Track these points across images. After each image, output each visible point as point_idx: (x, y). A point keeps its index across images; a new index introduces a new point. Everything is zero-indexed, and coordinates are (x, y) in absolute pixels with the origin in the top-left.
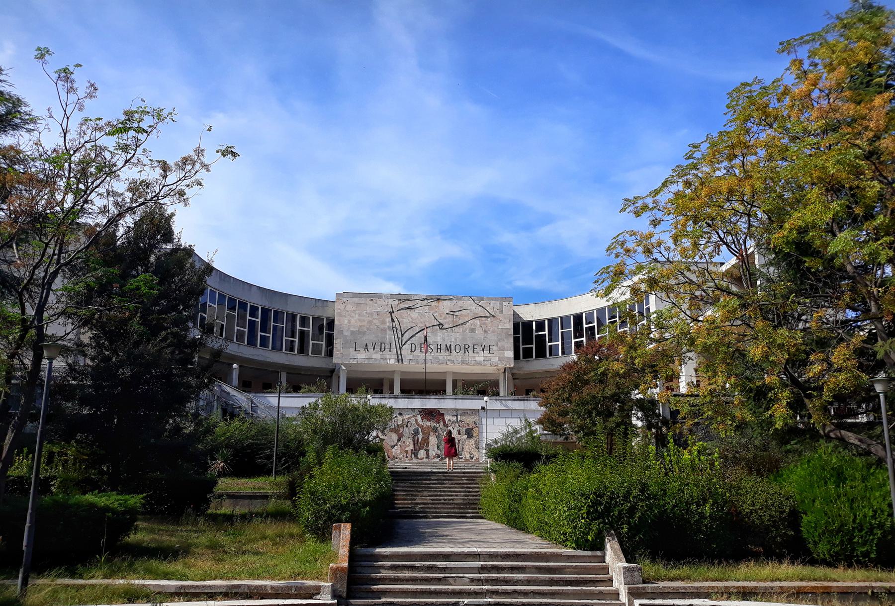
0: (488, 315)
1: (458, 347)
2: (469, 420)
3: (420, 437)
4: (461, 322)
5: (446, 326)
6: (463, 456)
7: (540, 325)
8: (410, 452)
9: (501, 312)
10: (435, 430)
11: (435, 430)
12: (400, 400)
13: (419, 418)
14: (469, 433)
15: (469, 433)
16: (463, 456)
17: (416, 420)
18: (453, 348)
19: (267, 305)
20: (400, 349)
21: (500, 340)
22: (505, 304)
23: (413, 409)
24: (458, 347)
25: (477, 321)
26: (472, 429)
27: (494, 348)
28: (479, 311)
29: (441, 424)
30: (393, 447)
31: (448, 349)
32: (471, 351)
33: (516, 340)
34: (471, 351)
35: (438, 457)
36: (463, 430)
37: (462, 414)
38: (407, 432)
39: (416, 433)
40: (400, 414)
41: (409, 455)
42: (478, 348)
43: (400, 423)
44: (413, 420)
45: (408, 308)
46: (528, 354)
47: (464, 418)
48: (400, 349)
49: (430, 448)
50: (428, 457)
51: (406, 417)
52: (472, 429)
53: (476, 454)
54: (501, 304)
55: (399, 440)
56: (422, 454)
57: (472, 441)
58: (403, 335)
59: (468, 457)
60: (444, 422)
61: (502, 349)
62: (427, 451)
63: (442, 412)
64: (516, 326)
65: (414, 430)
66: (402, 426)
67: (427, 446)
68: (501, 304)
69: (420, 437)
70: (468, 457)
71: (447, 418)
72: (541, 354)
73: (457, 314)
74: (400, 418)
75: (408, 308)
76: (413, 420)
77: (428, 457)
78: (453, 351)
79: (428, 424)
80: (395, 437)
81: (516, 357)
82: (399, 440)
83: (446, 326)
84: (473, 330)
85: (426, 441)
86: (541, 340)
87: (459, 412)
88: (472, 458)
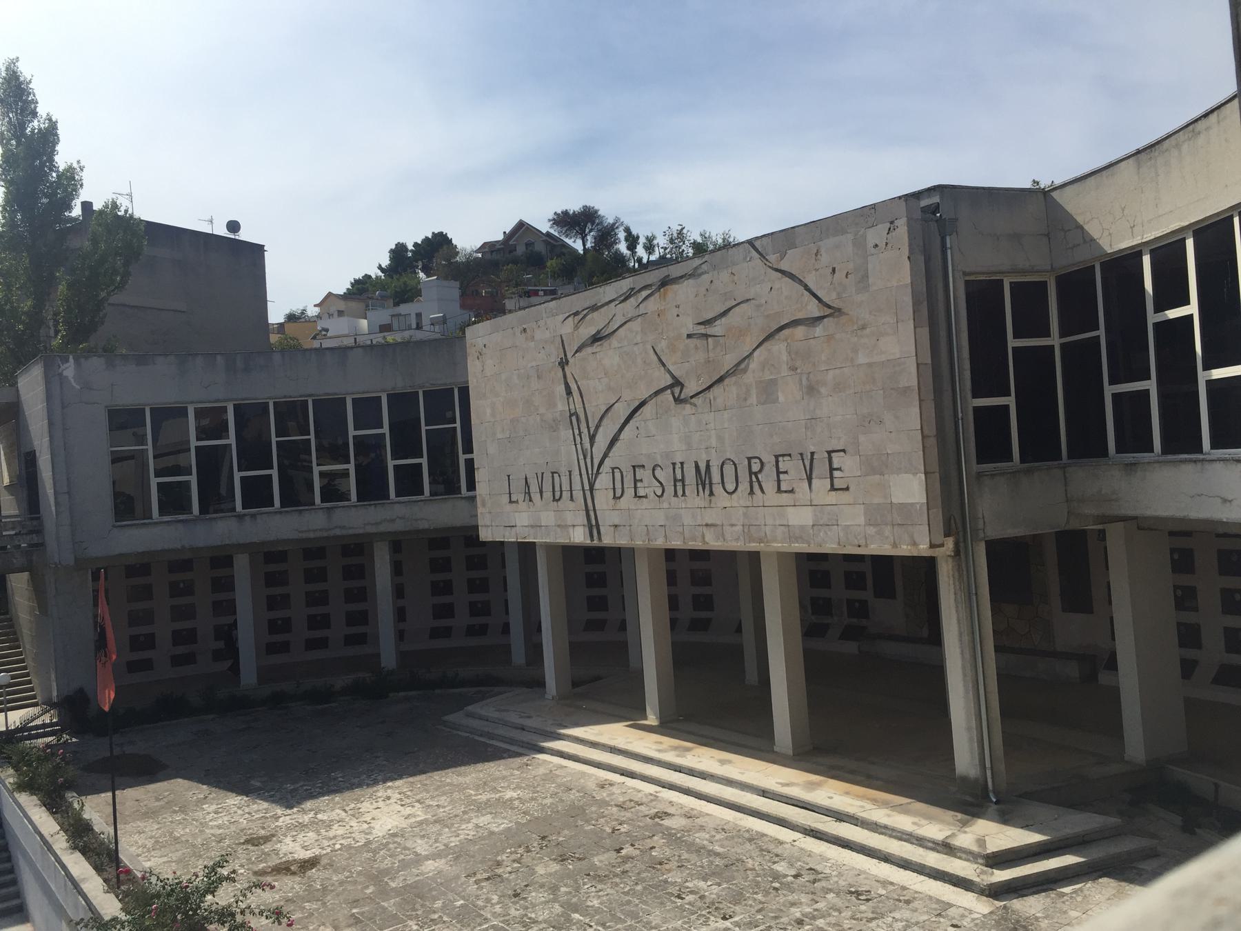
0: (814, 309)
4: (729, 361)
5: (692, 387)
18: (716, 477)
19: (400, 384)
20: (591, 489)
25: (778, 348)
31: (704, 479)
45: (596, 338)
48: (591, 489)
54: (859, 243)
58: (592, 438)
61: (878, 466)
68: (859, 243)
73: (717, 329)
75: (596, 338)
78: (718, 489)
83: (692, 387)
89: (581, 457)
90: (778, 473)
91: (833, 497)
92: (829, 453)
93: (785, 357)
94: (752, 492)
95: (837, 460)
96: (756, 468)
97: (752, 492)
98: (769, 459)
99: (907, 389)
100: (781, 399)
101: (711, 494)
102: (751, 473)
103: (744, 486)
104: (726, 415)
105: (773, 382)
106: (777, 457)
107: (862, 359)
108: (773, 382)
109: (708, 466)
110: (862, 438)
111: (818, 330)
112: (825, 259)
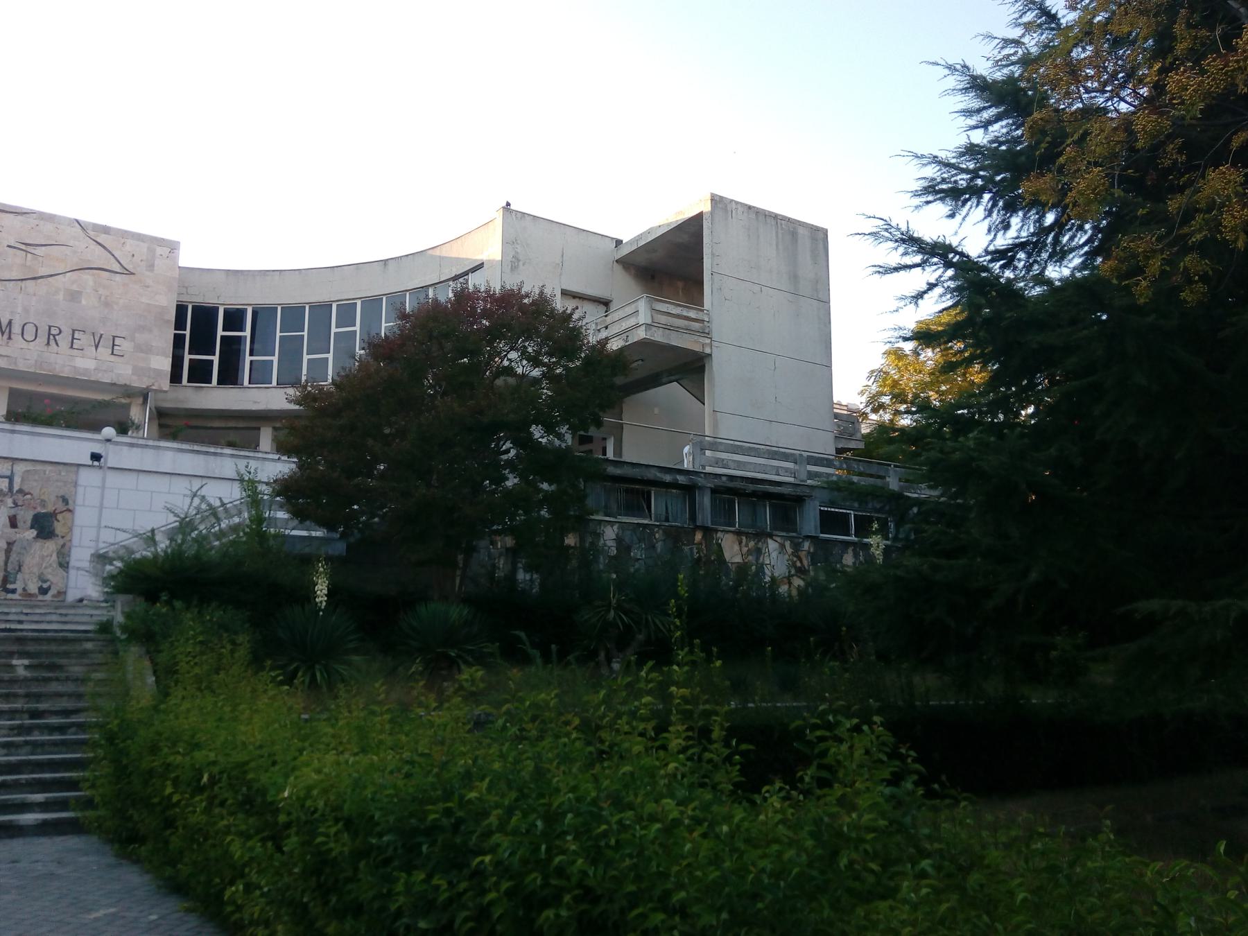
0: (117, 268)
1: (30, 330)
4: (43, 271)
6: (18, 586)
7: (234, 318)
9: (151, 267)
14: (44, 526)
16: (18, 586)
18: (16, 329)
21: (142, 329)
22: (159, 251)
24: (30, 330)
25: (87, 277)
26: (53, 515)
27: (124, 346)
28: (97, 257)
32: (64, 341)
33: (178, 341)
34: (64, 341)
36: (26, 516)
42: (84, 340)
46: (200, 374)
53: (55, 578)
57: (51, 546)
59: (33, 588)
61: (147, 350)
64: (181, 310)
70: (33, 588)
72: (229, 376)
73: (39, 251)
78: (17, 337)
81: (175, 377)
84: (74, 296)
86: (232, 350)
88: (44, 591)
90: (73, 338)
91: (113, 358)
92: (114, 337)
93: (91, 283)
94: (48, 343)
95: (117, 341)
96: (54, 331)
97: (48, 343)
98: (67, 332)
99: (168, 321)
100: (84, 302)
101: (10, 338)
102: (49, 334)
103: (42, 339)
105: (80, 293)
106: (74, 331)
107: (144, 300)
108: (80, 293)
109: (10, 323)
110: (137, 335)
111: (118, 277)
112: (128, 248)
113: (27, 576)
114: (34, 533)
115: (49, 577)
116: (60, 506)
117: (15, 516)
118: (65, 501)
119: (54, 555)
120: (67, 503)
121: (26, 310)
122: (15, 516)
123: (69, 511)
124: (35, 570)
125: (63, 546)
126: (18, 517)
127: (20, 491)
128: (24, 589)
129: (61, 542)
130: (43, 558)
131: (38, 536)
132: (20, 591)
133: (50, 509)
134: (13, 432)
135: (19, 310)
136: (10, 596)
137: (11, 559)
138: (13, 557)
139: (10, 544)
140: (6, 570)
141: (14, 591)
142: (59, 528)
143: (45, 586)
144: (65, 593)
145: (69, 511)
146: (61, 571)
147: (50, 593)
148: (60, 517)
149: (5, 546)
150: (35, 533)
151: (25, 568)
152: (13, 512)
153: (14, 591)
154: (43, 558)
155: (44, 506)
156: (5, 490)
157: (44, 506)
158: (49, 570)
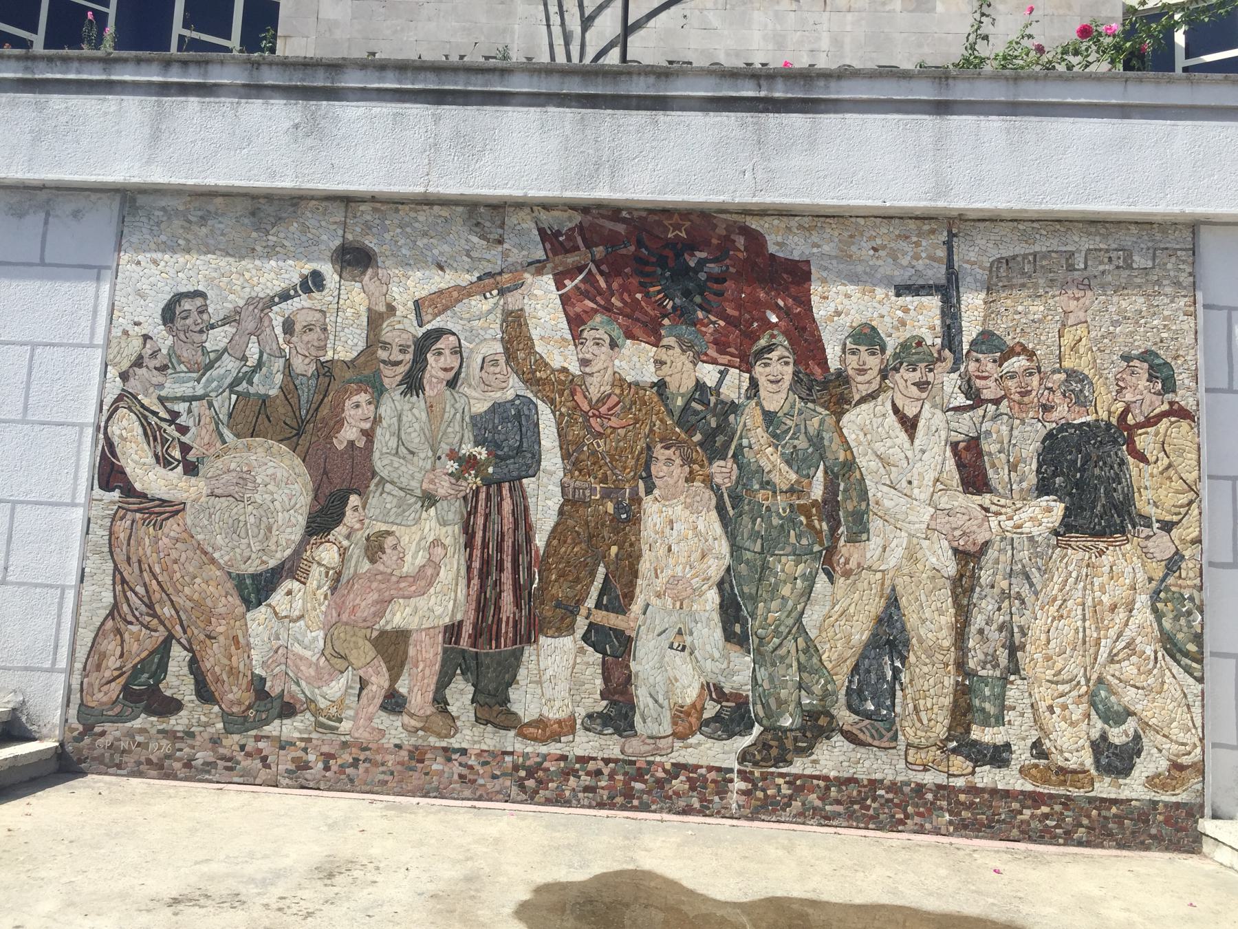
2: (1085, 338)
3: (545, 498)
6: (1015, 732)
8: (426, 655)
10: (706, 428)
11: (706, 428)
12: (351, 113)
13: (543, 301)
14: (1089, 481)
15: (1089, 481)
16: (1015, 732)
17: (515, 330)
23: (487, 215)
26: (1119, 433)
29: (777, 370)
30: (257, 589)
35: (731, 715)
36: (1018, 442)
37: (1003, 276)
38: (408, 438)
39: (505, 446)
40: (355, 259)
41: (416, 688)
43: (347, 345)
44: (477, 325)
47: (1029, 314)
49: (648, 617)
50: (618, 713)
51: (409, 286)
52: (1119, 433)
55: (323, 520)
56: (555, 675)
57: (1124, 567)
58: (587, 22)
59: (1072, 743)
60: (807, 345)
62: (614, 647)
63: (784, 243)
65: (483, 428)
66: (366, 374)
67: (618, 595)
69: (545, 498)
70: (1072, 743)
71: (838, 306)
74: (350, 299)
76: (477, 325)
77: (618, 713)
79: (637, 362)
80: (281, 481)
82: (323, 520)
85: (605, 543)
87: (974, 254)
88: (1116, 760)
89: (559, 41)
104: (849, 17)
113: (1044, 695)
114: (1046, 513)
115: (1129, 696)
116: (1142, 395)
117: (974, 444)
118: (1162, 374)
119: (1143, 615)
120: (1169, 385)
121: (837, 42)
122: (974, 444)
123: (1181, 413)
124: (1073, 667)
125: (1173, 564)
126: (989, 446)
127: (986, 341)
128: (1038, 749)
129: (1162, 546)
130: (1096, 613)
131: (1068, 527)
132: (1021, 755)
133: (1105, 407)
134: (942, 108)
135: (825, 44)
136: (987, 777)
137: (978, 621)
138: (985, 609)
139: (969, 558)
140: (961, 665)
141: (998, 756)
142: (1151, 490)
143: (1118, 736)
144: (1199, 769)
145: (1181, 413)
146: (1175, 677)
147: (1145, 767)
148: (1144, 441)
149: (951, 568)
150: (1059, 509)
151: (1031, 658)
152: (965, 424)
153: (998, 756)
154: (1096, 613)
155: (1081, 401)
156: (933, 339)
157: (1081, 401)
158: (1129, 669)
